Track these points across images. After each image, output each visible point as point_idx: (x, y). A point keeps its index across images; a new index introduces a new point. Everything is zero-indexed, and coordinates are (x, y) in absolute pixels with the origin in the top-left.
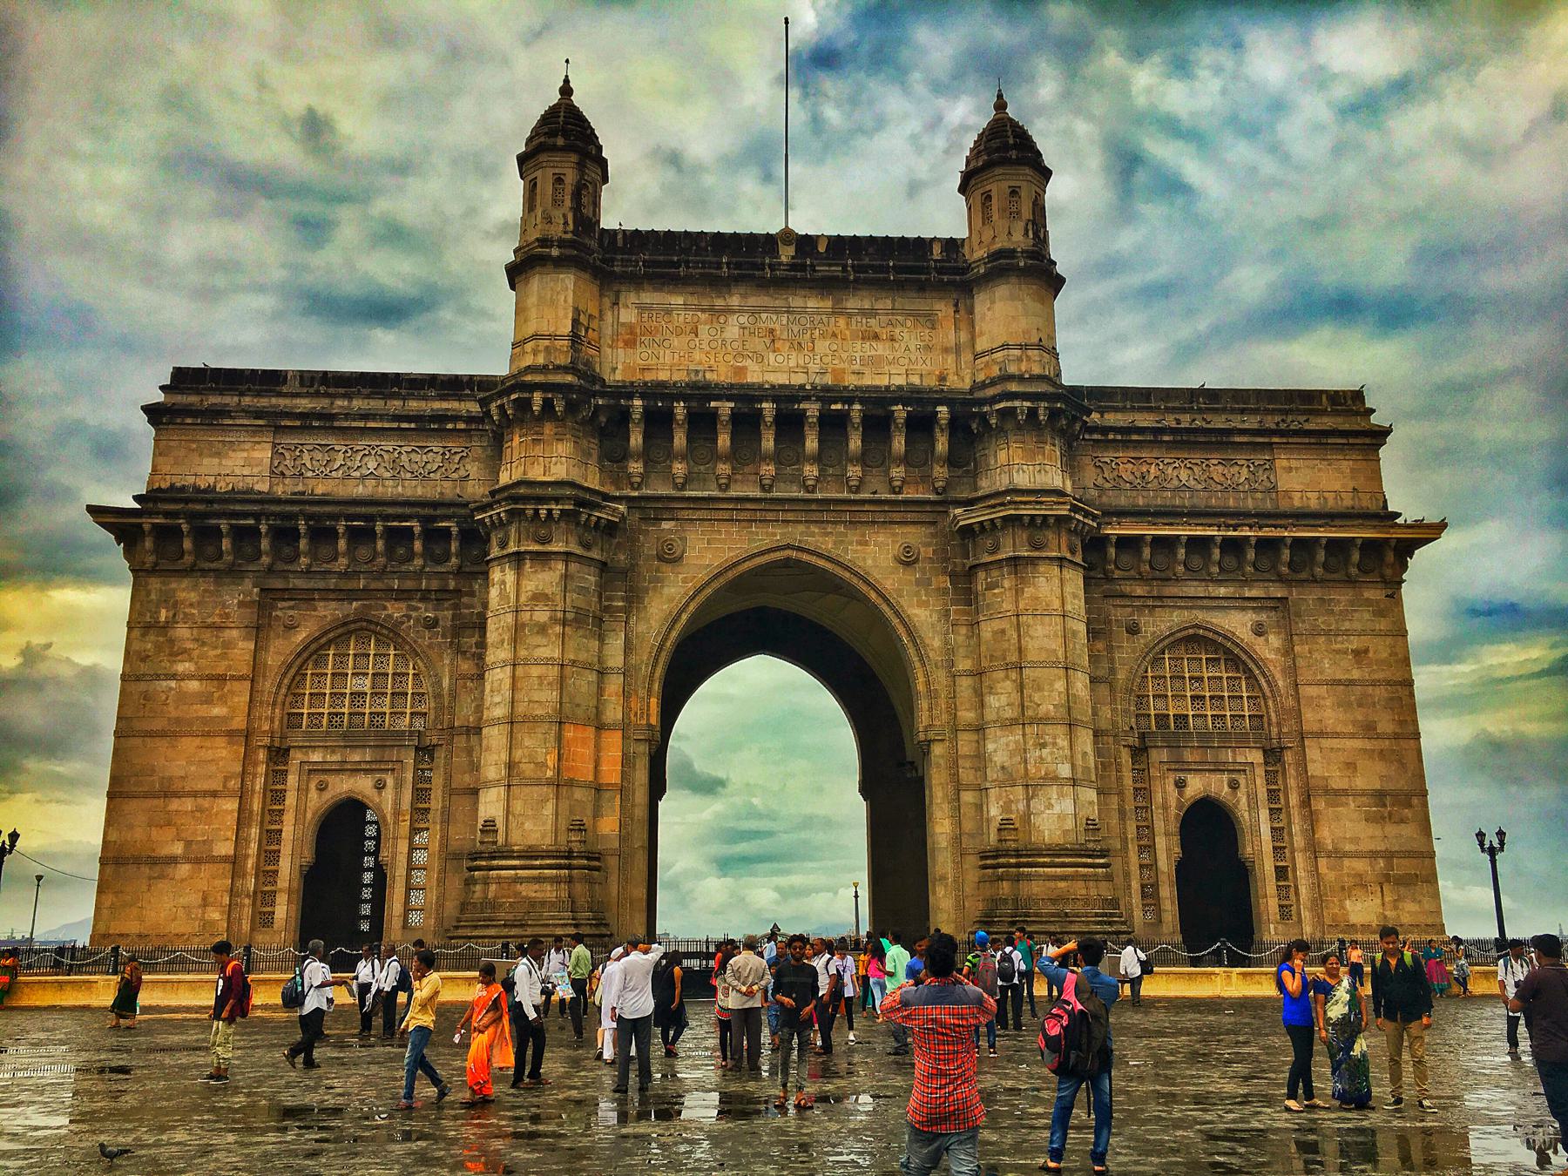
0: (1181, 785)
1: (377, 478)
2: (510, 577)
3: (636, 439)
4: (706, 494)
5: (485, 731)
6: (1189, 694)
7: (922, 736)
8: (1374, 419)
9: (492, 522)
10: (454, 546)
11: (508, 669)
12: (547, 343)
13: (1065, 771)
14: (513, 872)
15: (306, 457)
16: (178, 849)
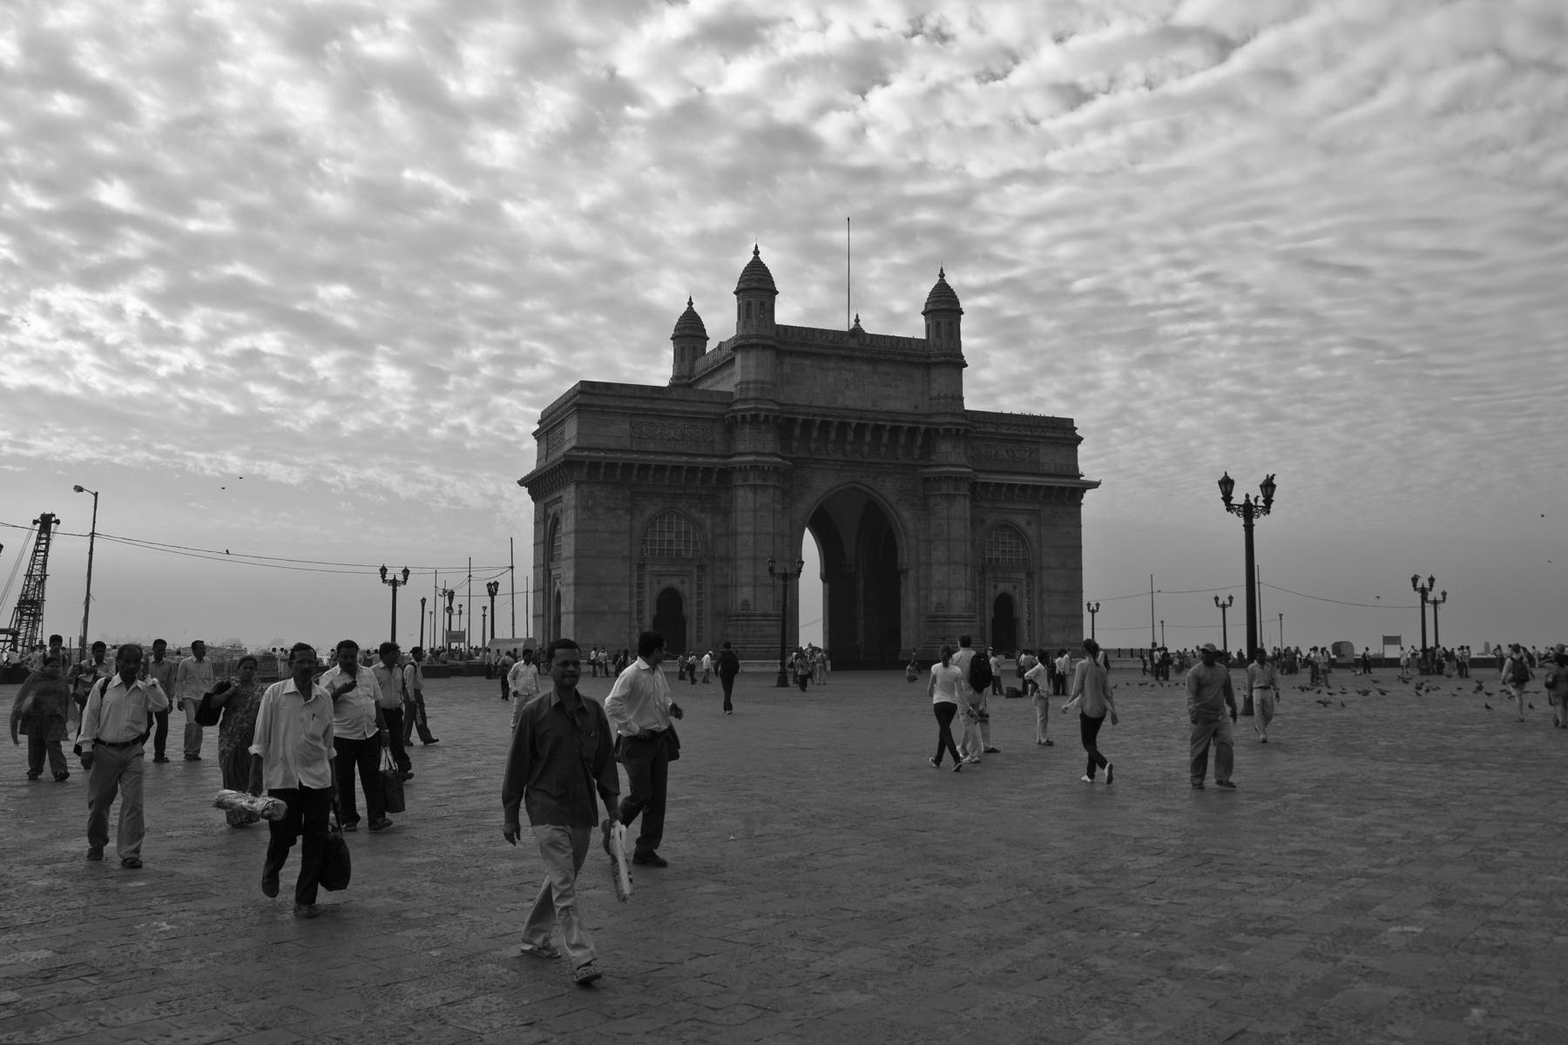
0: (996, 587)
1: (675, 440)
2: (750, 495)
3: (797, 432)
4: (822, 458)
5: (739, 562)
6: (1000, 549)
7: (904, 567)
8: (1076, 431)
9: (740, 470)
10: (715, 476)
11: (751, 536)
12: (760, 385)
13: (963, 585)
14: (758, 622)
15: (644, 427)
16: (606, 608)
